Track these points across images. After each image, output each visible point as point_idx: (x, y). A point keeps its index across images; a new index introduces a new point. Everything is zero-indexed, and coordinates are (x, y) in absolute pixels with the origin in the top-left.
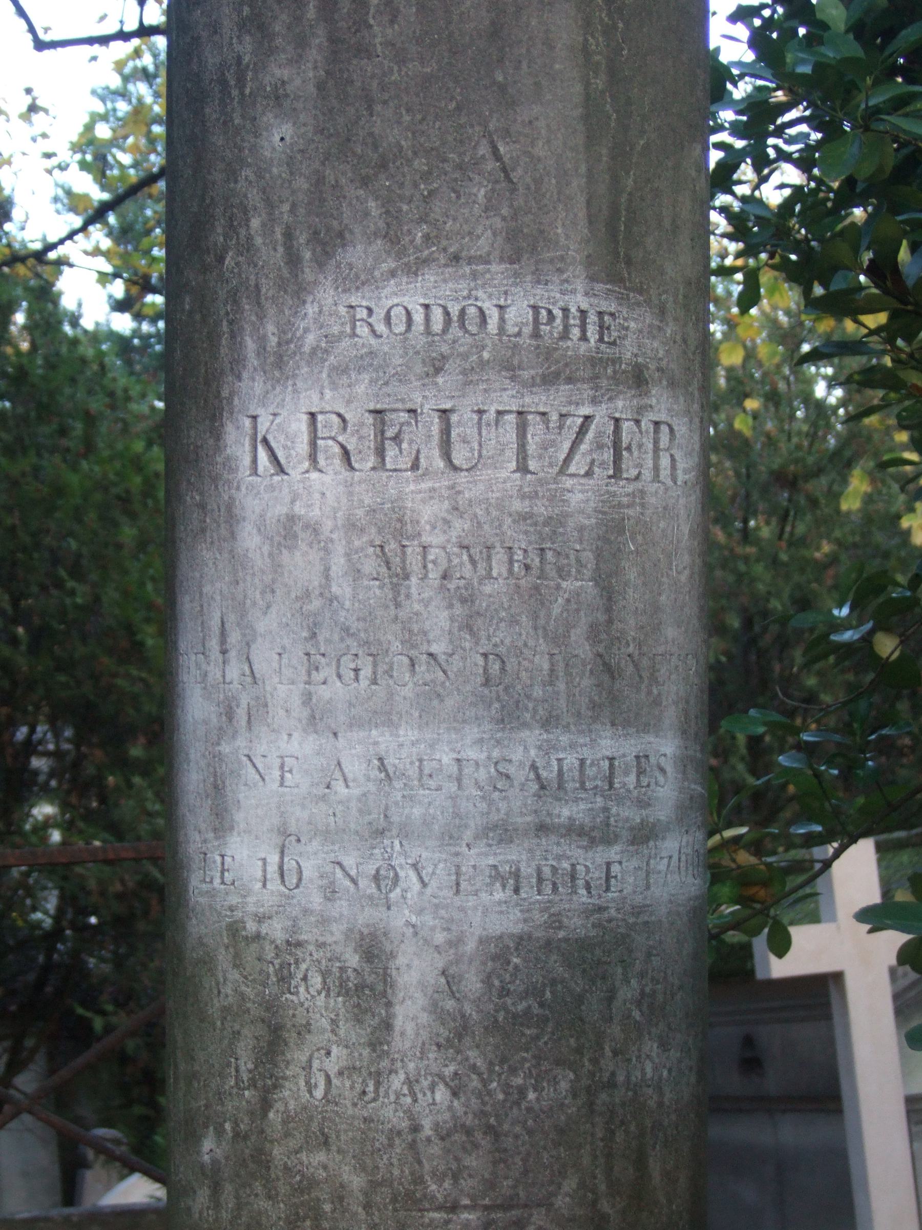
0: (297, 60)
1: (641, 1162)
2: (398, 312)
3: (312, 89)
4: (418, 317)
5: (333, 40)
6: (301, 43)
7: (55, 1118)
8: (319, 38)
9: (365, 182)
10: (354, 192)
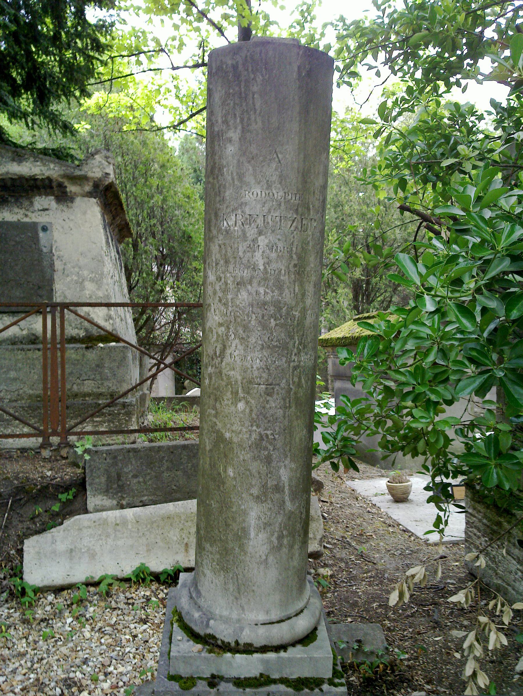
0: (235, 132)
1: (300, 378)
2: (255, 193)
3: (238, 139)
4: (259, 193)
5: (243, 128)
6: (236, 128)
7: (176, 369)
8: (240, 127)
9: (249, 162)
10: (246, 164)
